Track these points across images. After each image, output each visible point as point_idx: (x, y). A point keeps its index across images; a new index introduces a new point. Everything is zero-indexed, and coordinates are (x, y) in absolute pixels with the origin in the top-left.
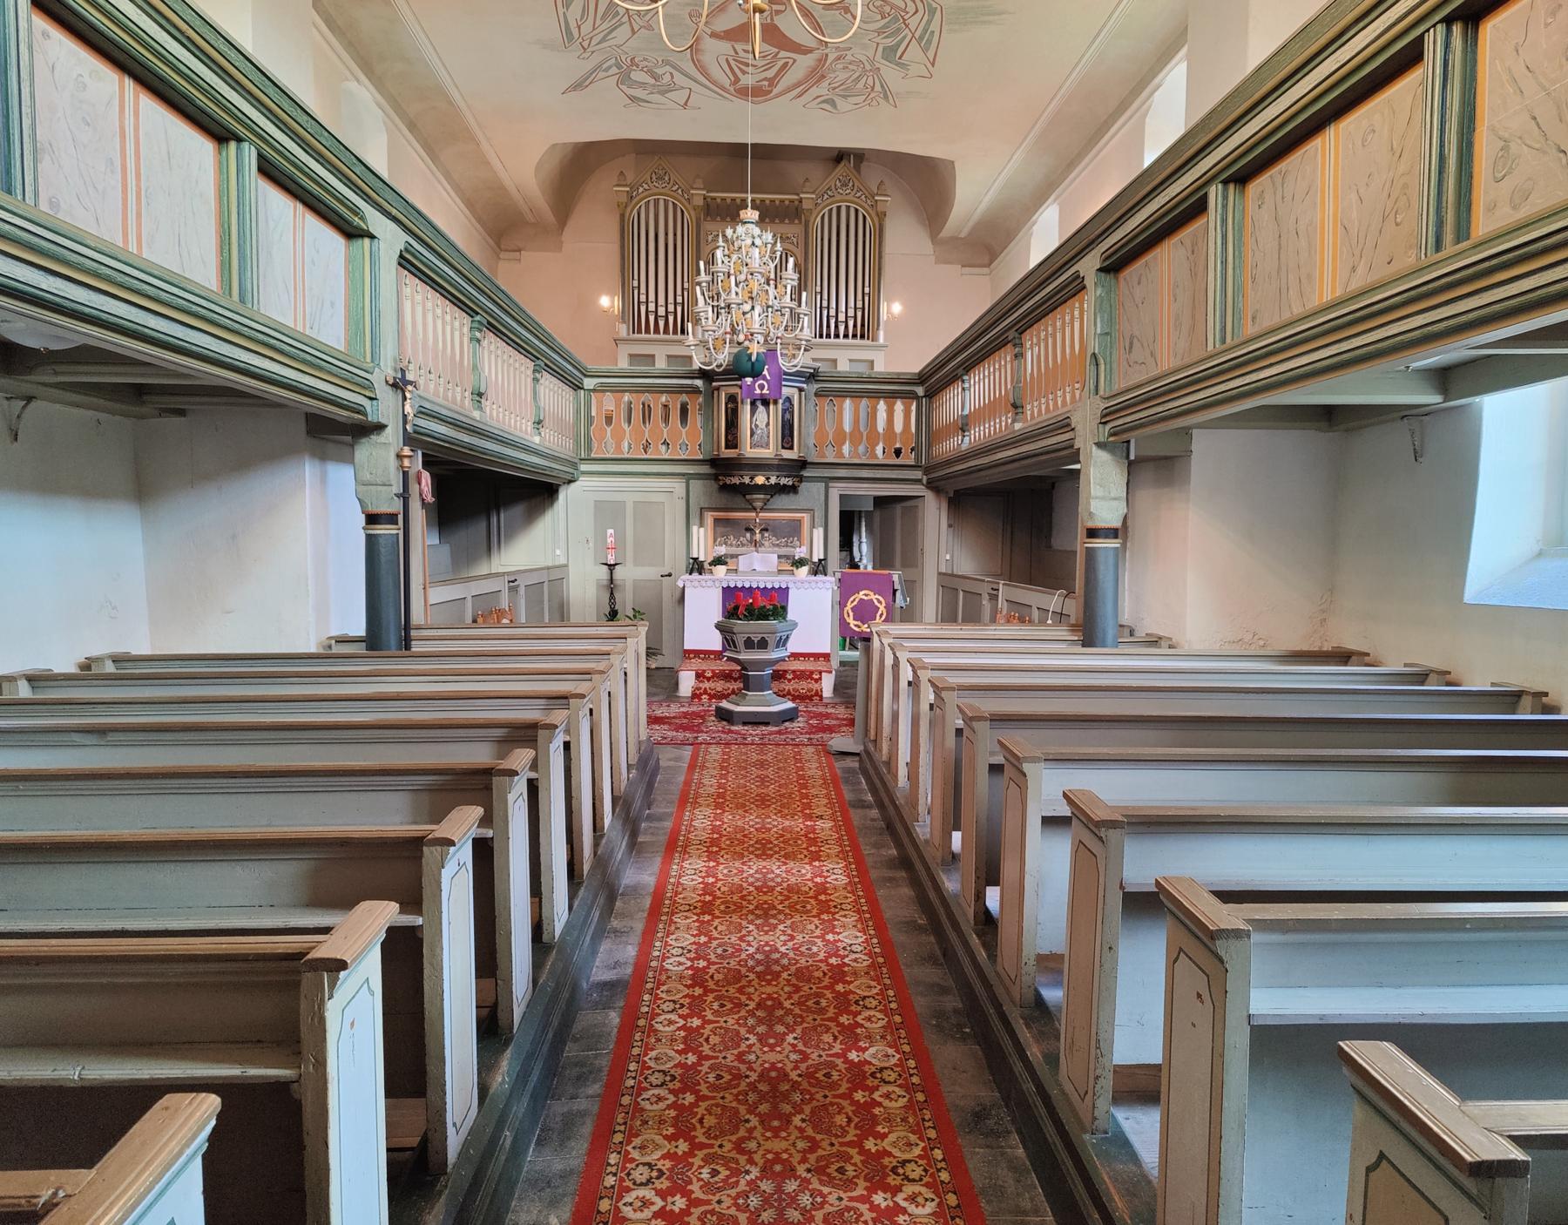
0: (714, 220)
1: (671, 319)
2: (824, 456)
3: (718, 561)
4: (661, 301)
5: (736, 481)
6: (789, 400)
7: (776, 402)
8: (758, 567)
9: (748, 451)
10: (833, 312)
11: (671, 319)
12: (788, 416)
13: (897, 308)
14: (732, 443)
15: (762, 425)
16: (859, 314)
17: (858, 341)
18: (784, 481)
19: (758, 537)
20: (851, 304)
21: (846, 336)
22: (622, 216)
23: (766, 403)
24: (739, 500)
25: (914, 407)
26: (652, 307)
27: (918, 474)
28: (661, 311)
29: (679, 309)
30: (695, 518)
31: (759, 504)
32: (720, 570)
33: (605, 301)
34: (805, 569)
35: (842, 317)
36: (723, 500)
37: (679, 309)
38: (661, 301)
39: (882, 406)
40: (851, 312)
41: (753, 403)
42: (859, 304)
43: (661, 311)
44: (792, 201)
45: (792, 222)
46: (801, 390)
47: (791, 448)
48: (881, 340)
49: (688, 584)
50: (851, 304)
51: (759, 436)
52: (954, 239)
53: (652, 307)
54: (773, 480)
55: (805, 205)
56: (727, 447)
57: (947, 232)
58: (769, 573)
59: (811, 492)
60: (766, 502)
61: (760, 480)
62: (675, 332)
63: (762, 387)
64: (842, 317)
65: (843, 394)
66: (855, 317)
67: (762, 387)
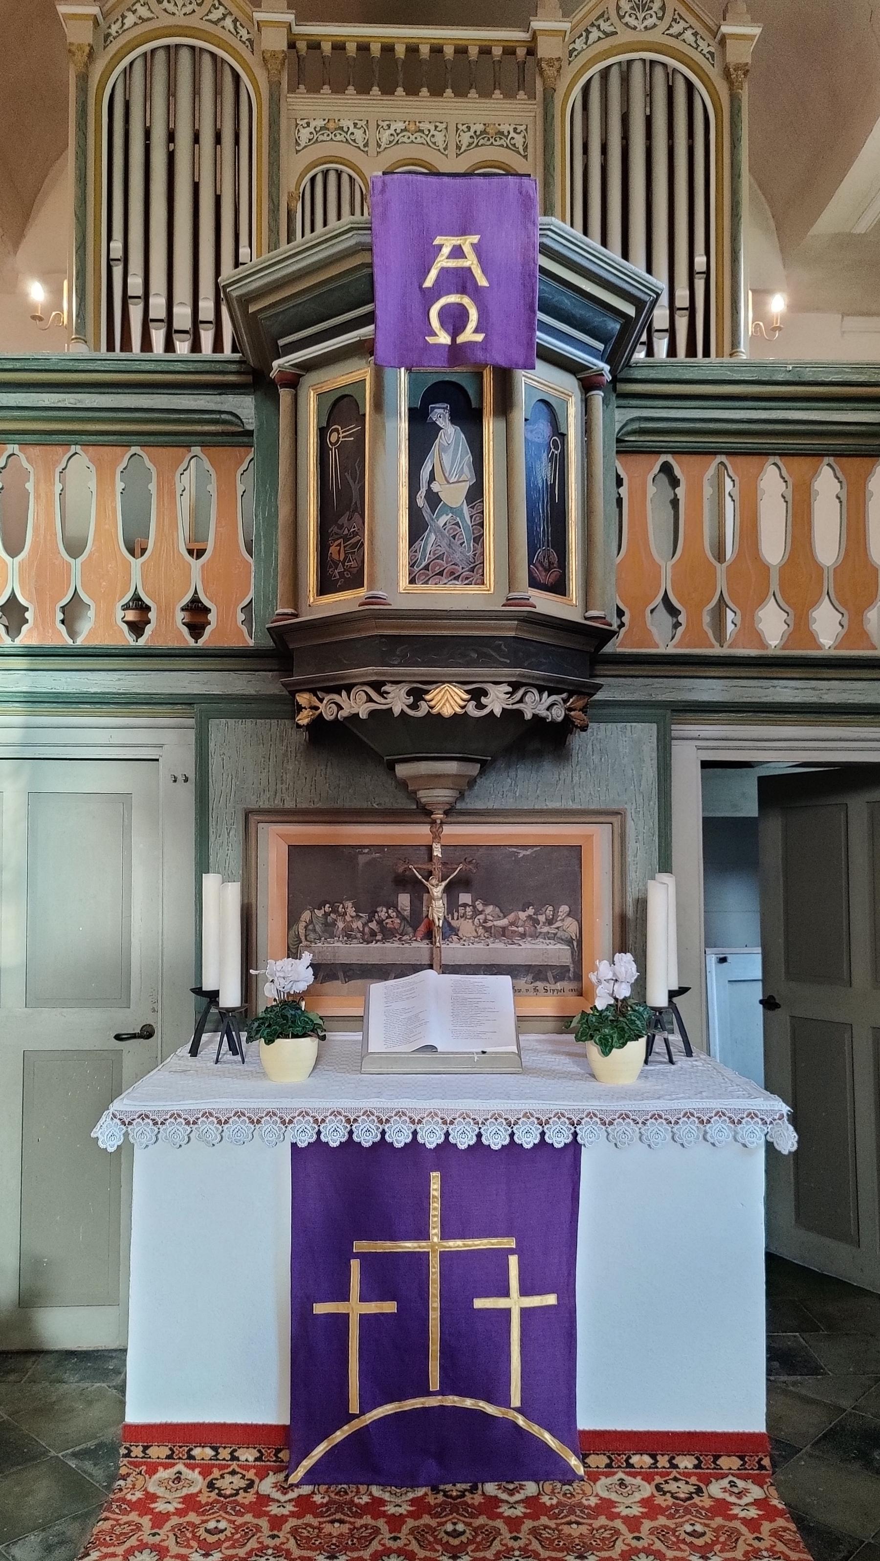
0: (314, 89)
2: (647, 638)
3: (288, 1020)
5: (357, 705)
6: (550, 411)
7: (505, 405)
8: (440, 1052)
9: (396, 582)
15: (453, 494)
16: (682, 324)
18: (536, 705)
19: (438, 909)
23: (469, 418)
26: (157, 305)
28: (182, 316)
30: (226, 845)
31: (441, 795)
33: (37, 292)
36: (324, 781)
39: (827, 483)
41: (419, 417)
43: (182, 316)
45: (510, 95)
46: (588, 385)
47: (559, 588)
52: (845, 242)
53: (157, 305)
54: (497, 700)
55: (546, 49)
56: (324, 588)
57: (832, 218)
59: (615, 753)
60: (465, 786)
61: (448, 700)
63: (455, 320)
65: (704, 443)
66: (672, 331)
67: (455, 320)
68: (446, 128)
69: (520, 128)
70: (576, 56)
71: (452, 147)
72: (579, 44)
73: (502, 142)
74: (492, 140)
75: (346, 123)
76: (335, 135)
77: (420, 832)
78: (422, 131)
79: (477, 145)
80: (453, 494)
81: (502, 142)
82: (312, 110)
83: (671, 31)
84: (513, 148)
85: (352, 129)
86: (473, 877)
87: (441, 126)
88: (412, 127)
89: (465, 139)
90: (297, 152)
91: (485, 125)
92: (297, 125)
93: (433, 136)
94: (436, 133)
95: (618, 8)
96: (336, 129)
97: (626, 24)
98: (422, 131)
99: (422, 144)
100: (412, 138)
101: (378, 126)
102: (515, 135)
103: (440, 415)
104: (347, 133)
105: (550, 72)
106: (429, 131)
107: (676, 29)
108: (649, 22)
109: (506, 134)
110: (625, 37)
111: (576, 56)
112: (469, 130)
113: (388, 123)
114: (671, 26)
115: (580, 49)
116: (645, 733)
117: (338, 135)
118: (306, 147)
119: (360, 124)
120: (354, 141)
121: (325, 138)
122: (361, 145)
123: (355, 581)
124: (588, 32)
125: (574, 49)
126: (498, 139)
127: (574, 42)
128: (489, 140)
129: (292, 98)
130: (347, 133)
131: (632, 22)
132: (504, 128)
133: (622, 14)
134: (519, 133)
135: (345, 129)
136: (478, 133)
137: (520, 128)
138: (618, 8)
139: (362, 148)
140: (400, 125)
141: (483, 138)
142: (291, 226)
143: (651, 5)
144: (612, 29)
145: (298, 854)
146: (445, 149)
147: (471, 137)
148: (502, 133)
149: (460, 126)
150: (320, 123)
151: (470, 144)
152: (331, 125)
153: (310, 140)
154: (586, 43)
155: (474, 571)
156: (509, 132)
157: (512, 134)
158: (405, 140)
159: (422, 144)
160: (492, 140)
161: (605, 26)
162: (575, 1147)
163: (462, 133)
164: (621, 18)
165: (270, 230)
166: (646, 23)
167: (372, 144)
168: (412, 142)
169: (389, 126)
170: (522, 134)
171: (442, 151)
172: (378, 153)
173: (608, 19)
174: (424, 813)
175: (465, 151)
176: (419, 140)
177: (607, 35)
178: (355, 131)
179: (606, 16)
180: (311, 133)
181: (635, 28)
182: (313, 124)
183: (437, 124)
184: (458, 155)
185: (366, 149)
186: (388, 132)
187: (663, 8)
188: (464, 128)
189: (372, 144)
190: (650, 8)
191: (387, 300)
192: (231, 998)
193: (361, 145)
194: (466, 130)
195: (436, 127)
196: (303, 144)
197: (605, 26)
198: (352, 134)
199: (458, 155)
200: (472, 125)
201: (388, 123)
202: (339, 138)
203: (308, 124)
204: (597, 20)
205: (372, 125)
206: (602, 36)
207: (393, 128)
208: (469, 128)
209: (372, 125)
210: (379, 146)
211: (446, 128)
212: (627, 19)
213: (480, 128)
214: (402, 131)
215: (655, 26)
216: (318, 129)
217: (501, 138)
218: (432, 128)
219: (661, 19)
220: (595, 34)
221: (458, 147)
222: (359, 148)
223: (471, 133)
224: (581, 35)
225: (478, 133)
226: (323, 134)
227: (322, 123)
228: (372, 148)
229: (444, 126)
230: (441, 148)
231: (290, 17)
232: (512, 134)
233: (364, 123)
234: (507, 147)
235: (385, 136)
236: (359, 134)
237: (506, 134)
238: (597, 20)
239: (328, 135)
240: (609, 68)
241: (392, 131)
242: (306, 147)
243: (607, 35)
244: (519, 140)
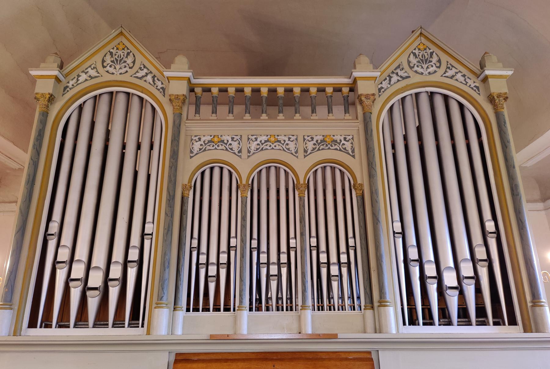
37: (132, 273)
44: (338, 89)
55: (363, 88)
68: (297, 139)
69: (348, 138)
70: (383, 92)
71: (301, 151)
72: (385, 85)
73: (336, 147)
74: (329, 146)
75: (225, 138)
76: (218, 146)
78: (280, 141)
79: (319, 150)
81: (336, 147)
83: (447, 74)
84: (345, 150)
85: (230, 142)
87: (293, 138)
88: (273, 139)
89: (310, 146)
90: (191, 157)
91: (323, 136)
92: (192, 140)
93: (287, 144)
94: (289, 142)
95: (409, 62)
96: (219, 142)
97: (416, 72)
98: (280, 141)
99: (280, 150)
100: (273, 146)
101: (249, 139)
102: (345, 142)
104: (226, 144)
105: (367, 102)
106: (285, 141)
107: (450, 73)
108: (431, 70)
109: (339, 141)
111: (383, 92)
112: (313, 140)
113: (255, 136)
114: (446, 71)
115: (385, 87)
117: (220, 146)
118: (197, 154)
119: (236, 138)
120: (231, 149)
121: (211, 148)
122: (236, 152)
124: (390, 77)
125: (382, 88)
126: (333, 145)
127: (381, 83)
128: (327, 146)
129: (189, 124)
130: (226, 144)
131: (420, 70)
132: (338, 138)
133: (412, 65)
134: (348, 141)
135: (226, 142)
136: (319, 141)
137: (348, 138)
138: (409, 62)
139: (237, 153)
140: (264, 138)
141: (323, 145)
142: (184, 208)
143: (431, 59)
144: (406, 75)
146: (296, 152)
147: (314, 144)
148: (336, 141)
149: (306, 137)
150: (208, 138)
151: (314, 149)
152: (216, 139)
153: (200, 149)
154: (390, 84)
156: (341, 141)
157: (343, 142)
158: (268, 147)
159: (280, 150)
160: (329, 146)
161: (401, 73)
163: (307, 142)
164: (411, 68)
165: (166, 213)
166: (429, 70)
167: (244, 151)
168: (273, 149)
169: (256, 139)
170: (350, 142)
171: (294, 154)
172: (249, 156)
173: (403, 69)
175: (310, 153)
176: (277, 147)
177: (403, 78)
178: (233, 143)
179: (401, 67)
180: (201, 145)
181: (422, 74)
182: (203, 139)
183: (290, 136)
184: (305, 156)
185: (240, 154)
186: (256, 143)
187: (439, 61)
188: (309, 138)
189: (244, 151)
190: (431, 61)
193: (236, 152)
194: (310, 140)
195: (289, 138)
196: (195, 152)
197: (401, 73)
198: (231, 144)
199: (305, 156)
200: (314, 137)
201: (255, 136)
202: (221, 147)
203: (200, 139)
204: (395, 69)
205: (245, 138)
206: (400, 79)
207: (259, 140)
208: (312, 138)
209: (245, 138)
210: (249, 152)
211: (297, 139)
212: (416, 68)
213: (320, 138)
214: (266, 141)
215: (435, 72)
216: (206, 142)
217: (335, 145)
218: (287, 139)
219: (439, 67)
220: (395, 78)
221: (305, 151)
222: (235, 153)
223: (314, 142)
224: (386, 79)
225: (319, 141)
226: (210, 145)
227: (209, 138)
228: (244, 154)
229: (295, 137)
230: (293, 152)
231: (189, 74)
232: (343, 142)
233: (238, 137)
234: (340, 150)
235: (254, 146)
236: (235, 145)
237: (339, 141)
238: (395, 69)
239: (213, 146)
240: (405, 97)
241: (258, 142)
242: (197, 154)
243: (403, 78)
244: (348, 145)
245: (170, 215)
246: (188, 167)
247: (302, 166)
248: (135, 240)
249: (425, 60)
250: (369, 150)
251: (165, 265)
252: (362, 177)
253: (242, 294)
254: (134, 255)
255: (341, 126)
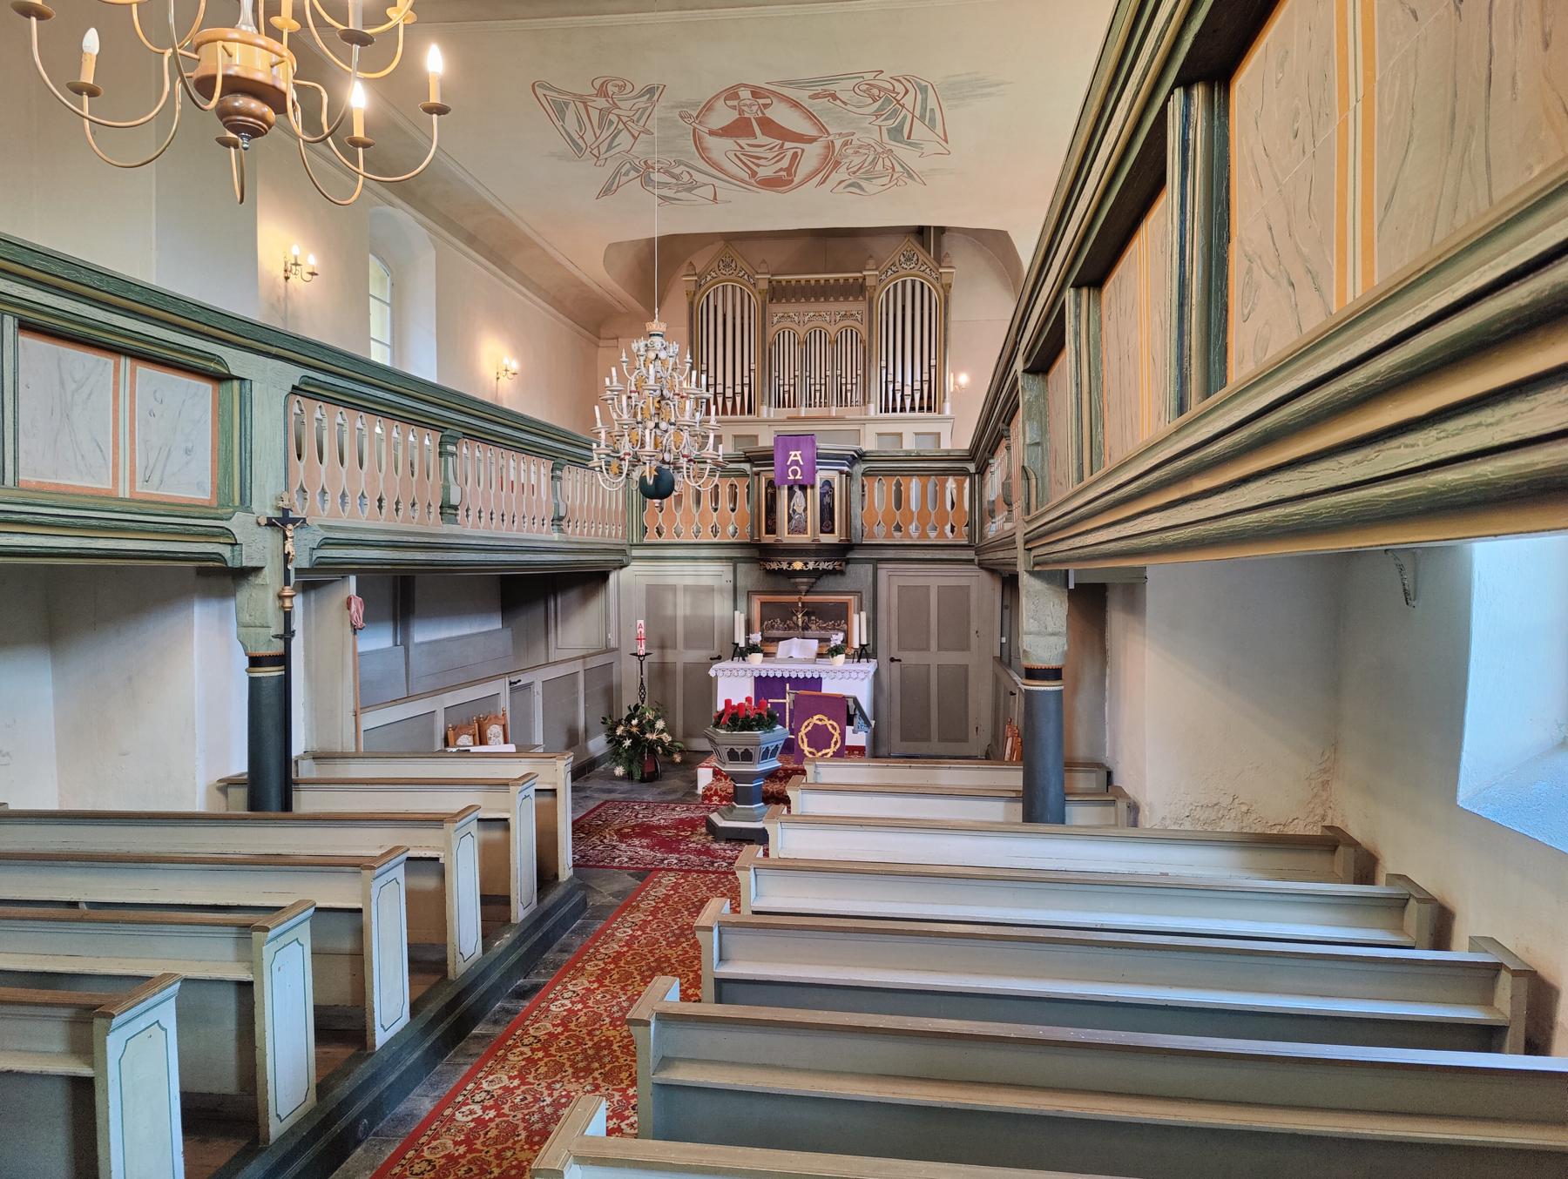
0: (779, 301)
1: (738, 399)
4: (729, 383)
5: (774, 566)
6: (828, 483)
7: (813, 487)
9: (785, 536)
10: (898, 386)
11: (738, 399)
12: (827, 499)
13: (964, 379)
14: (771, 529)
15: (800, 510)
17: (925, 414)
18: (823, 566)
20: (917, 377)
21: (912, 409)
22: (691, 304)
23: (803, 488)
24: (784, 584)
25: (967, 484)
27: (970, 554)
28: (729, 393)
29: (746, 389)
32: (756, 659)
34: (841, 657)
35: (908, 391)
37: (746, 389)
38: (729, 383)
40: (917, 385)
41: (790, 488)
42: (926, 377)
43: (729, 393)
44: (856, 279)
45: (856, 299)
47: (832, 531)
48: (948, 412)
49: (720, 673)
50: (917, 377)
51: (798, 517)
54: (811, 566)
55: (869, 282)
58: (806, 661)
61: (798, 565)
62: (742, 413)
64: (908, 391)
77: (794, 598)
80: (800, 510)
82: (778, 309)
86: (811, 611)
103: (796, 489)
110: (902, 272)
116: (870, 567)
123: (774, 532)
145: (763, 604)
155: (804, 531)
162: (820, 679)
174: (799, 592)
191: (778, 460)
192: (742, 644)
245: (764, 359)
246: (771, 331)
247: (833, 330)
248: (746, 373)
249: (909, 260)
250: (870, 321)
251: (763, 385)
252: (866, 337)
253: (801, 397)
254: (746, 380)
255: (857, 307)
